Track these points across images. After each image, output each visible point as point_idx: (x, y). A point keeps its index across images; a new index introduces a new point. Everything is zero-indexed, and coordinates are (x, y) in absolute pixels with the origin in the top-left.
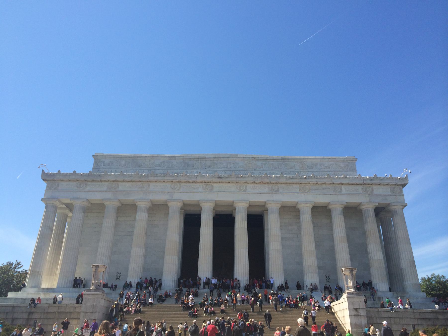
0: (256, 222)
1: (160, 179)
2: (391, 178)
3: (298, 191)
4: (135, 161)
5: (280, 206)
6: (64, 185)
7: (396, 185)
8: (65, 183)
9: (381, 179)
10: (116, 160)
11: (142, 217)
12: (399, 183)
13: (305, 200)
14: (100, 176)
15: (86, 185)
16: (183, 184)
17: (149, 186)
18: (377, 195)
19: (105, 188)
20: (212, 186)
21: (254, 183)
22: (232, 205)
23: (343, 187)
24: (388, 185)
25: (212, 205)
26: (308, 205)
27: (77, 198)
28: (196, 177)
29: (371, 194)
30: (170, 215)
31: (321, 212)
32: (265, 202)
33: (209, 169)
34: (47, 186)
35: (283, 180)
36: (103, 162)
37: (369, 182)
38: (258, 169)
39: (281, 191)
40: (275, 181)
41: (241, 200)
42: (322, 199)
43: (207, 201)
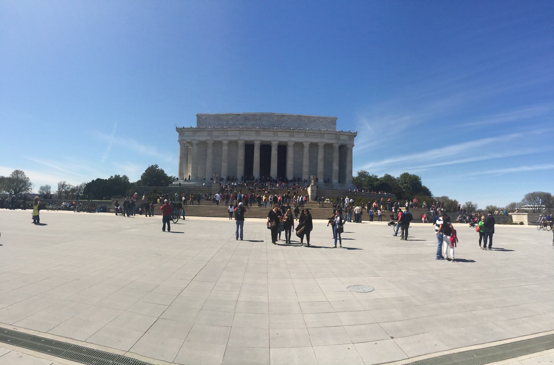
1: (233, 129)
2: (350, 132)
4: (218, 117)
6: (187, 134)
9: (345, 132)
10: (208, 116)
11: (225, 148)
13: (307, 140)
14: (203, 128)
27: (194, 140)
29: (338, 139)
31: (314, 146)
35: (297, 131)
40: (292, 131)
42: (314, 140)
43: (257, 140)
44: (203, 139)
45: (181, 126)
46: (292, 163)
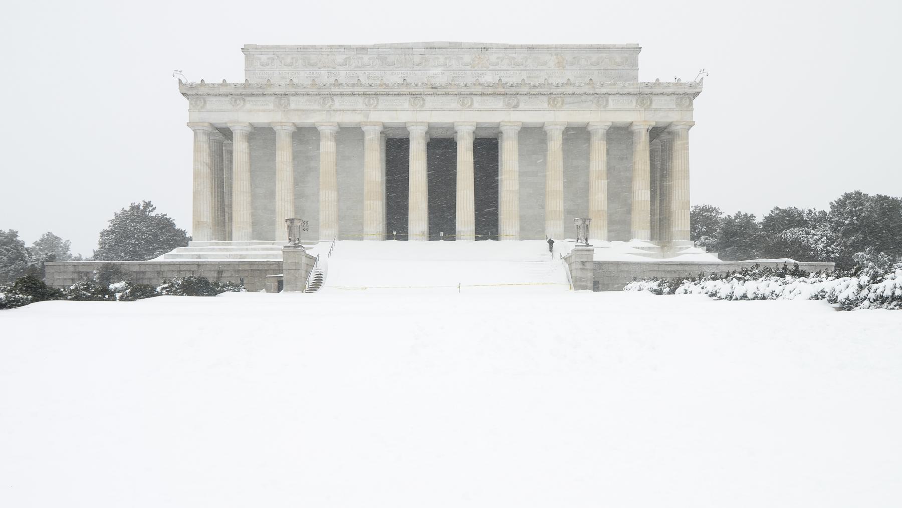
0: (487, 148)
3: (546, 105)
5: (519, 129)
8: (214, 99)
10: (277, 52)
11: (328, 147)
13: (557, 119)
15: (244, 100)
16: (380, 98)
17: (333, 100)
18: (656, 110)
19: (271, 106)
20: (424, 100)
21: (482, 94)
22: (451, 128)
25: (424, 129)
26: (558, 127)
28: (400, 85)
30: (367, 143)
31: (577, 135)
32: (499, 123)
34: (191, 104)
36: (260, 59)
37: (647, 90)
38: (491, 67)
39: (522, 106)
41: (464, 121)
43: (417, 123)
44: (262, 119)
45: (193, 78)
46: (516, 187)
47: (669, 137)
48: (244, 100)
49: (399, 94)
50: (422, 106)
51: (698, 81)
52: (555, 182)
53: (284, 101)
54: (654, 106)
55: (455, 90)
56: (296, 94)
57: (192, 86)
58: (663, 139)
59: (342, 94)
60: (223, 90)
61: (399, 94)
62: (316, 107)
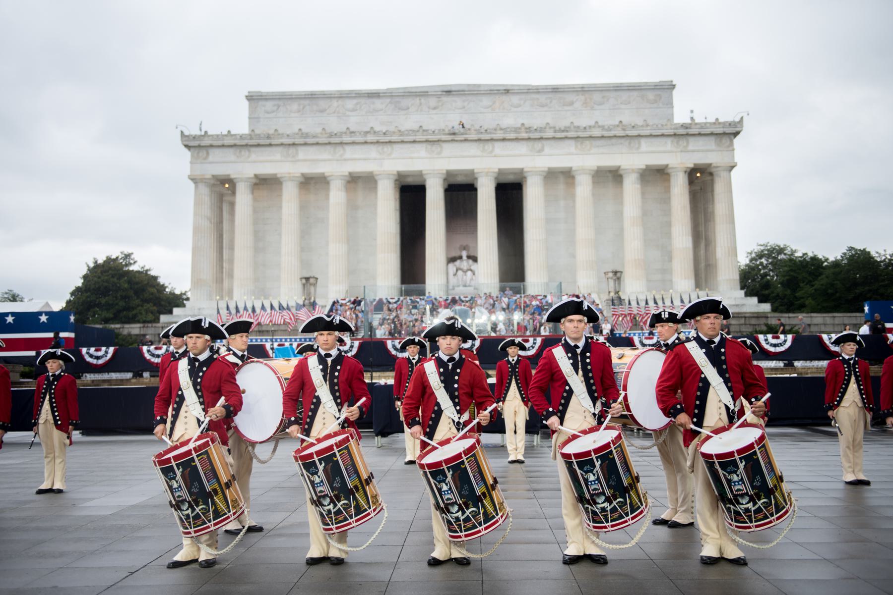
3: (573, 149)
7: (724, 134)
12: (728, 130)
16: (396, 146)
18: (693, 151)
21: (504, 140)
23: (643, 141)
24: (712, 134)
33: (435, 112)
34: (192, 156)
37: (682, 131)
39: (547, 150)
44: (266, 170)
47: (709, 178)
48: (249, 151)
49: (414, 142)
50: (439, 153)
51: (737, 120)
52: (584, 231)
53: (292, 150)
54: (691, 147)
55: (474, 136)
56: (305, 144)
57: (195, 138)
58: (701, 181)
59: (353, 143)
60: (227, 142)
61: (414, 142)
62: (326, 156)
